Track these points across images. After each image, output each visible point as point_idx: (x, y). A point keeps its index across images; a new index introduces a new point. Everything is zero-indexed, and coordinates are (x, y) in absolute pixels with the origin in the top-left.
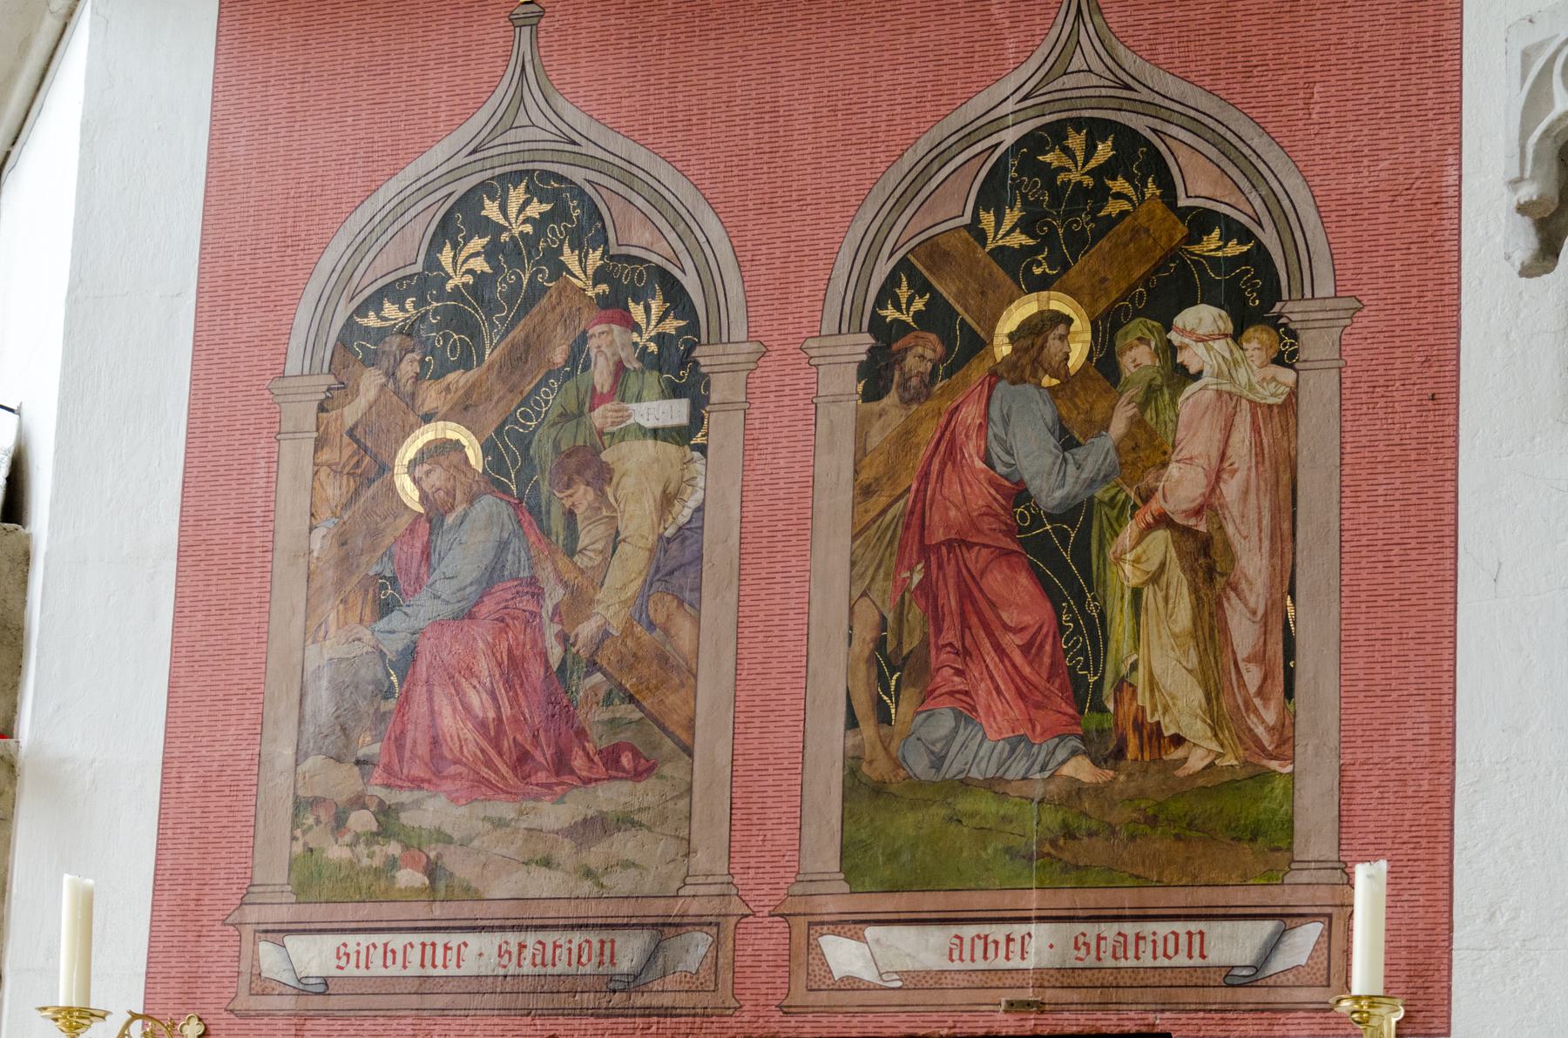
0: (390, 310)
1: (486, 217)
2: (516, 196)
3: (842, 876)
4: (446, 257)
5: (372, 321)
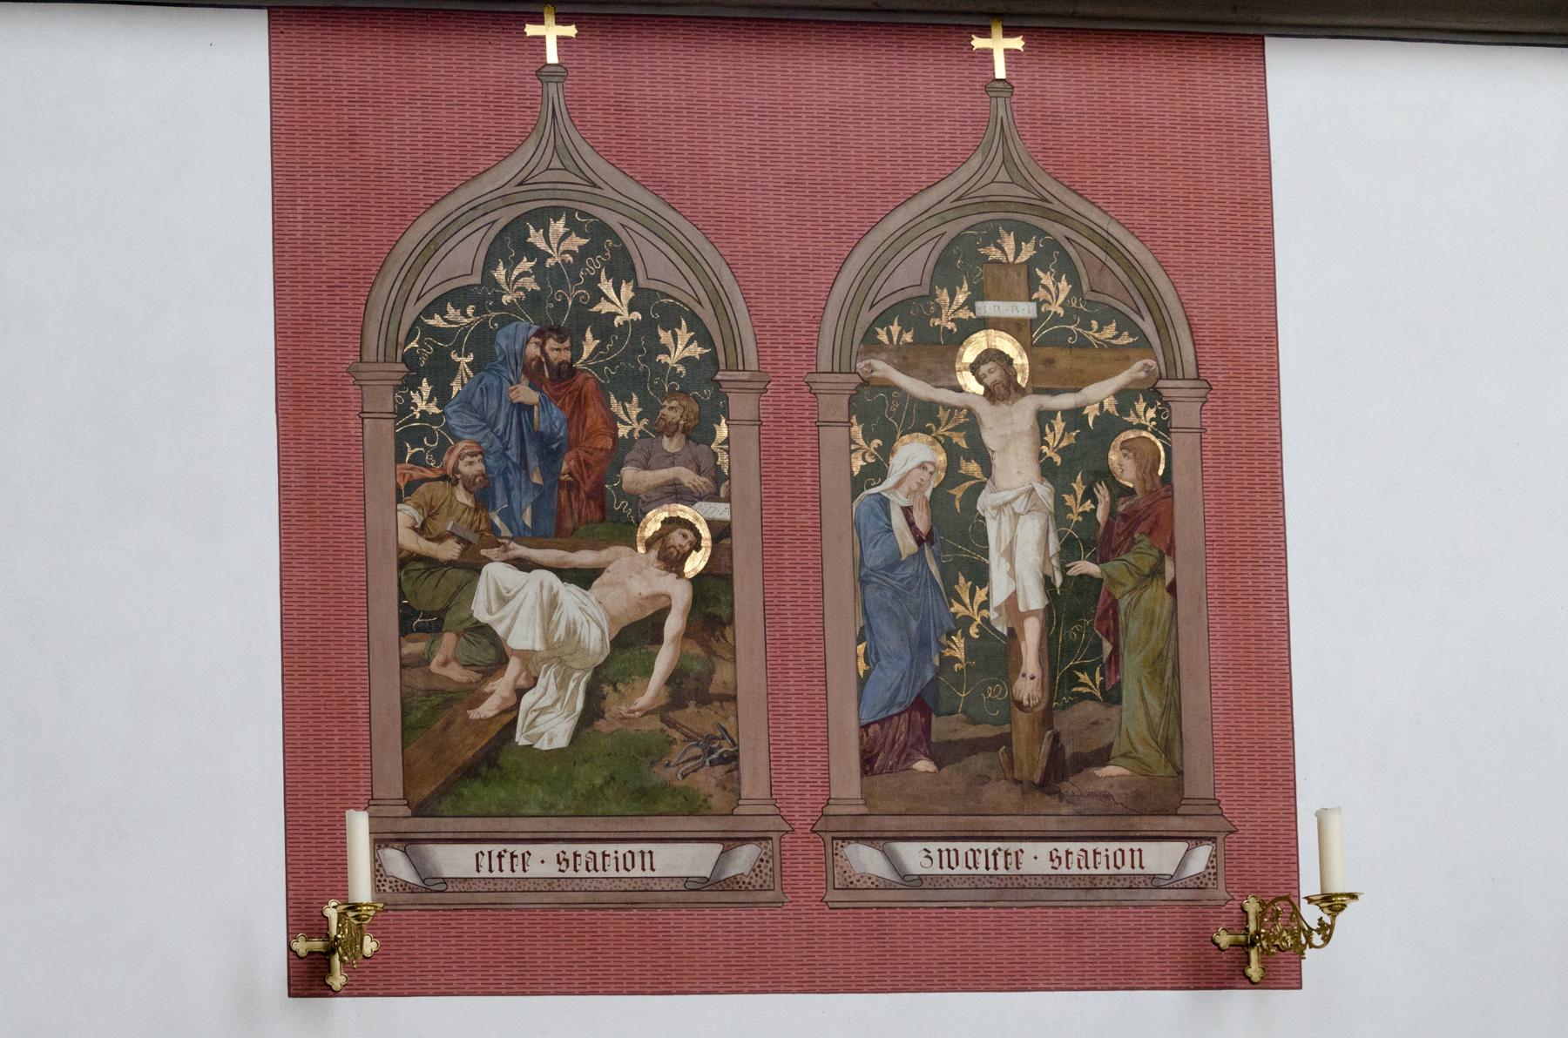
0: (452, 312)
1: (532, 243)
2: (559, 227)
3: (863, 802)
4: (500, 274)
5: (437, 321)
